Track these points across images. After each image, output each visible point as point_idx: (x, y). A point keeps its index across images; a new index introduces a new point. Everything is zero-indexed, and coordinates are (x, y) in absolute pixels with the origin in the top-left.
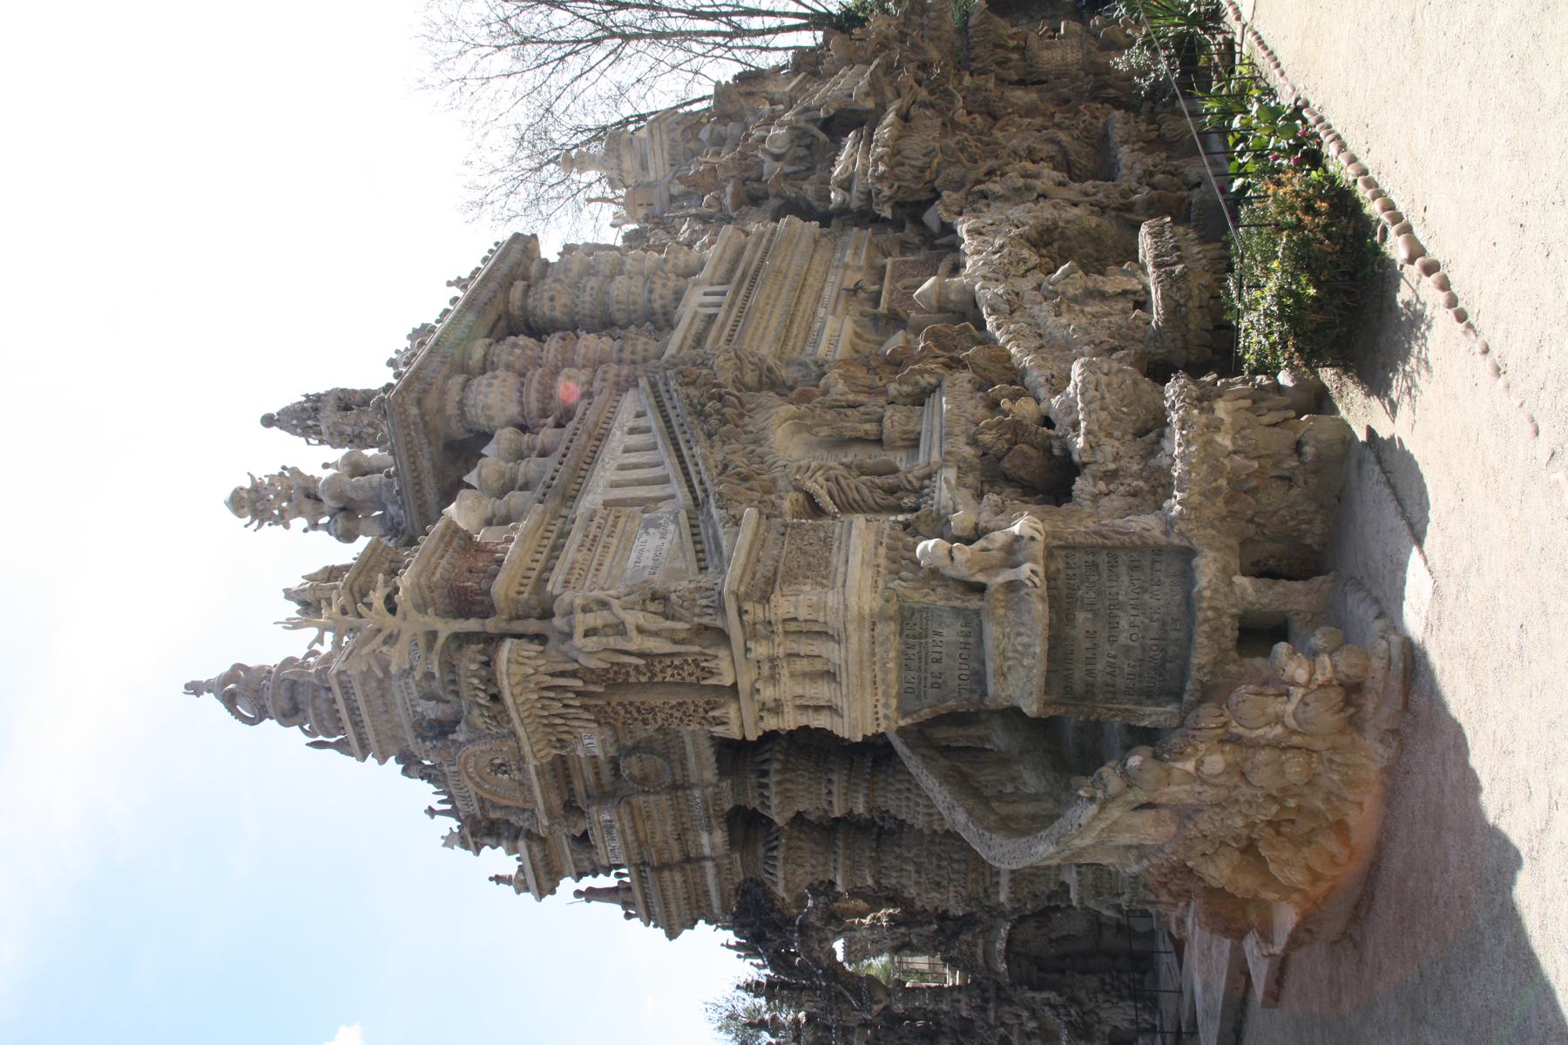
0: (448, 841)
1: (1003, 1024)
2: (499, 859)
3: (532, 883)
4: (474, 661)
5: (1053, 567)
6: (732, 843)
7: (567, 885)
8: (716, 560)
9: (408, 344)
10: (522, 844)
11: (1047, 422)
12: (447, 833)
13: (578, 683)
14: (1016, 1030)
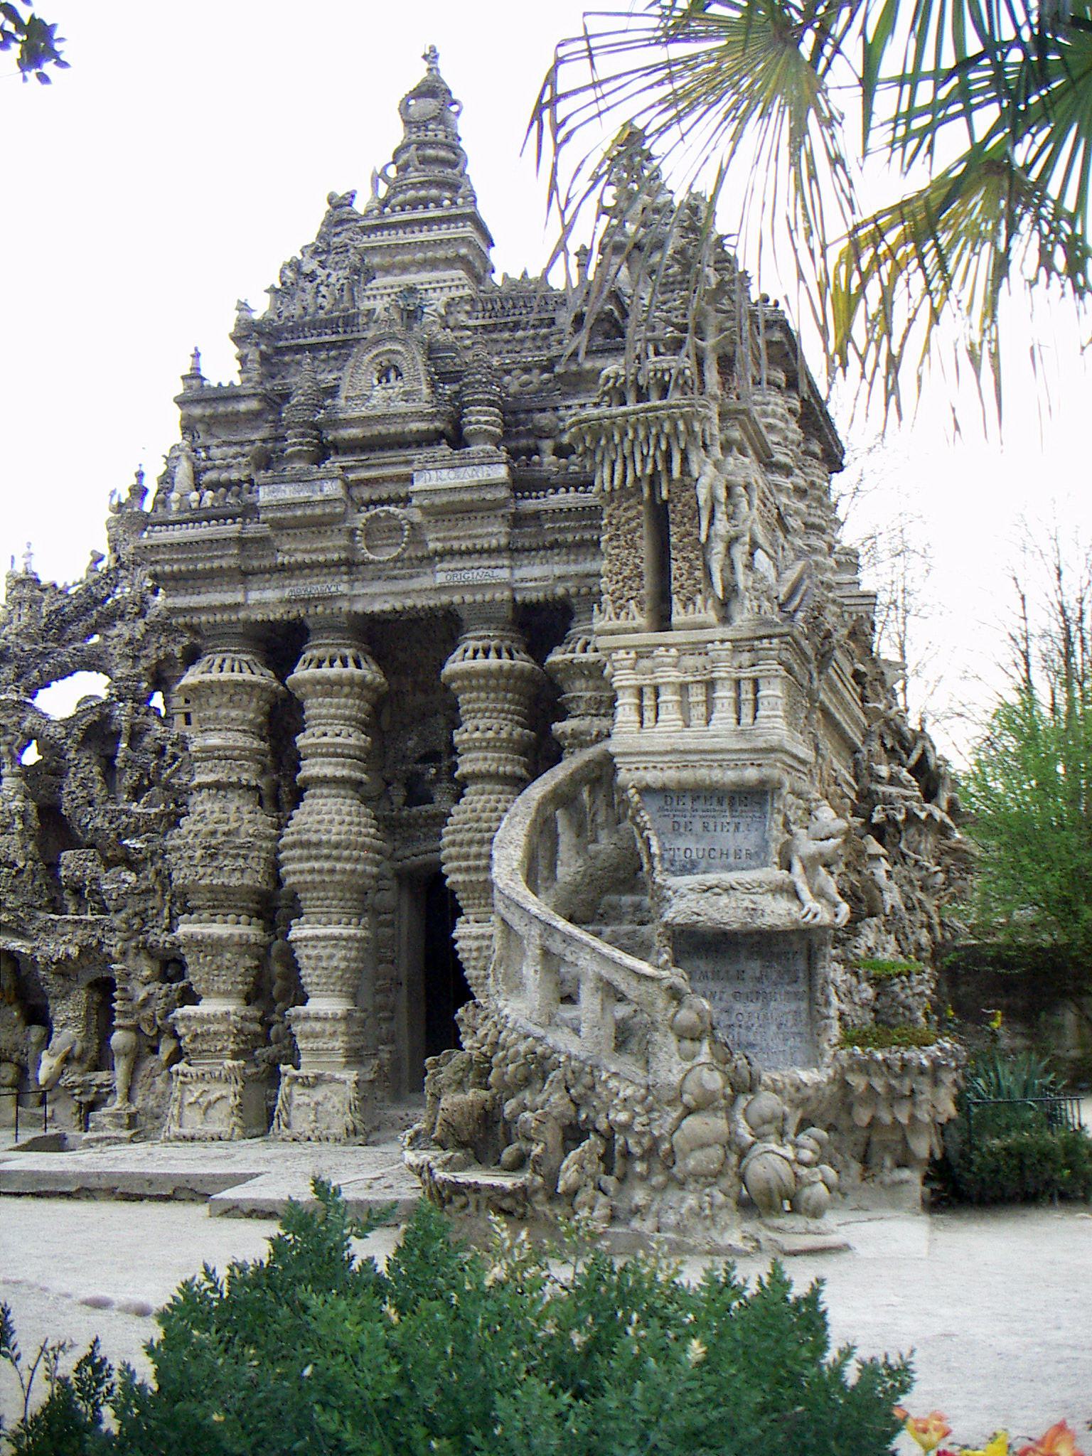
0: (243, 307)
5: (794, 938)
12: (251, 305)
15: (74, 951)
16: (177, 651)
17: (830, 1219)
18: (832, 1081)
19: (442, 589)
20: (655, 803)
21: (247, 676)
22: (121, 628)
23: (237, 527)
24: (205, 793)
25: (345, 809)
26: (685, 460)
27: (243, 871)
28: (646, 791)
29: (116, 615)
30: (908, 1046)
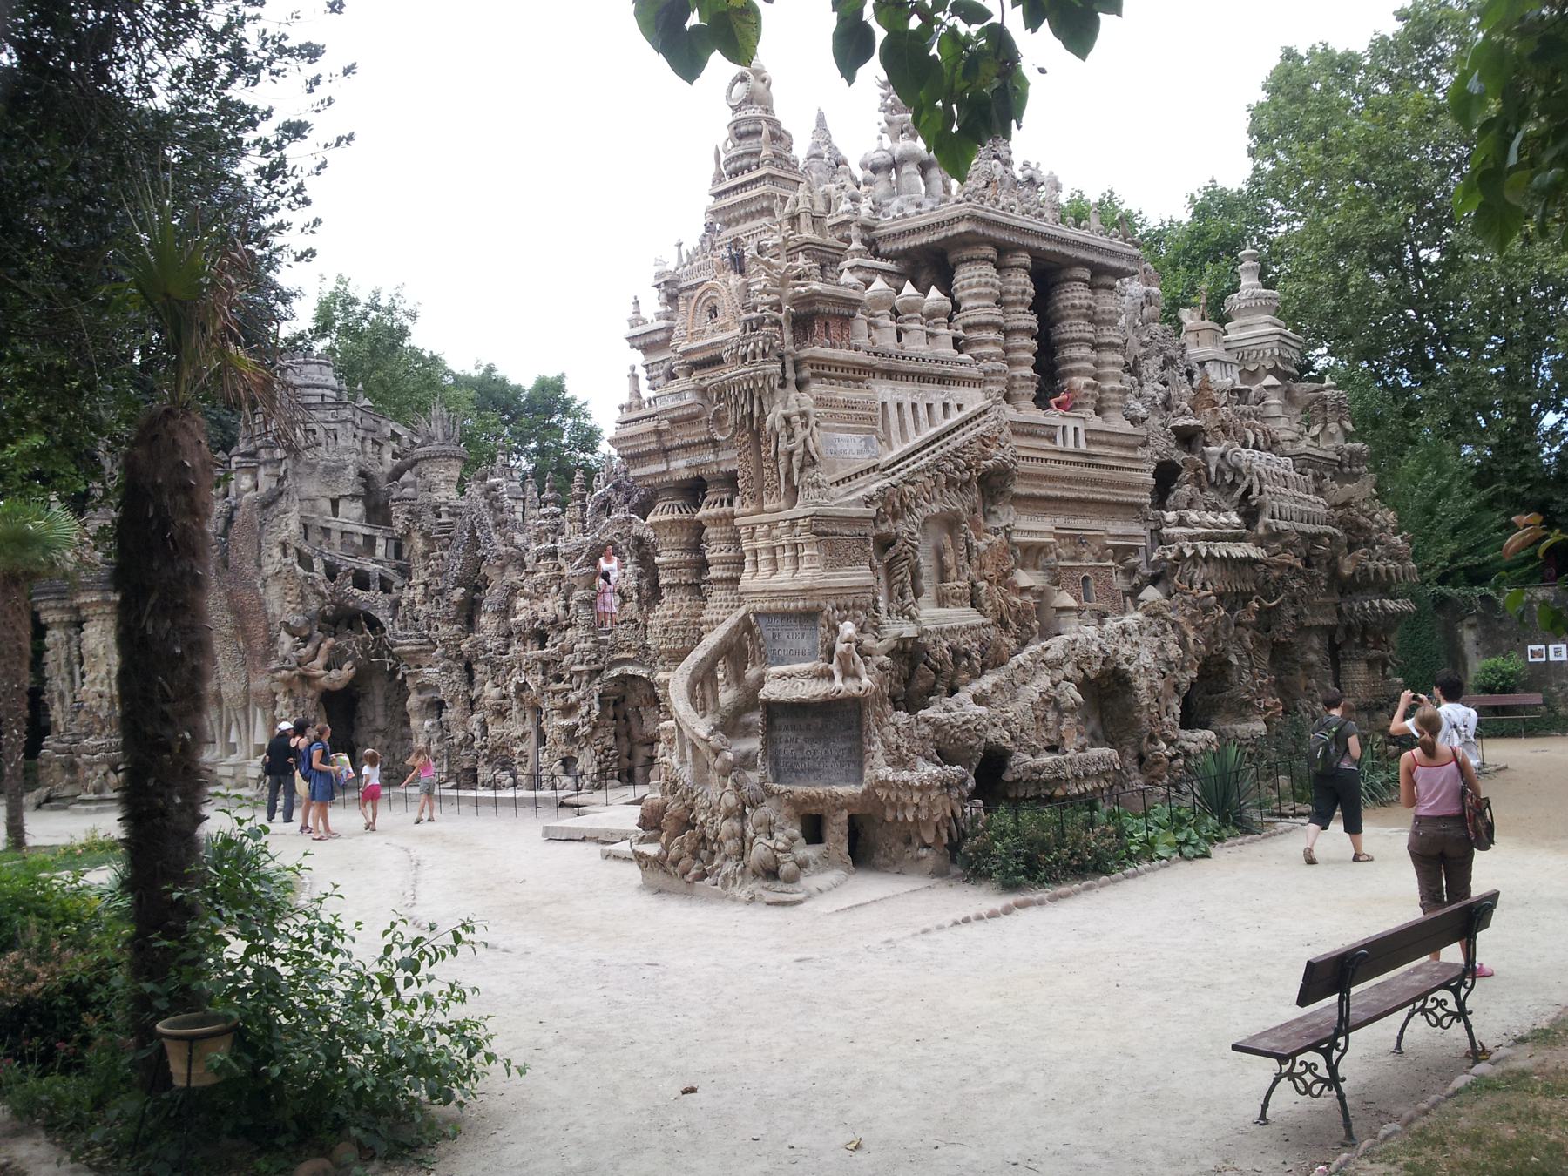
1: (572, 676)
2: (652, 305)
3: (637, 331)
4: (764, 343)
6: (681, 481)
7: (638, 358)
8: (842, 493)
9: (1046, 173)
10: (663, 323)
11: (953, 691)
13: (756, 414)
14: (568, 686)
17: (803, 881)
18: (864, 793)
20: (763, 621)
21: (677, 516)
23: (655, 423)
25: (730, 598)
26: (761, 404)
27: (683, 639)
30: (830, 784)
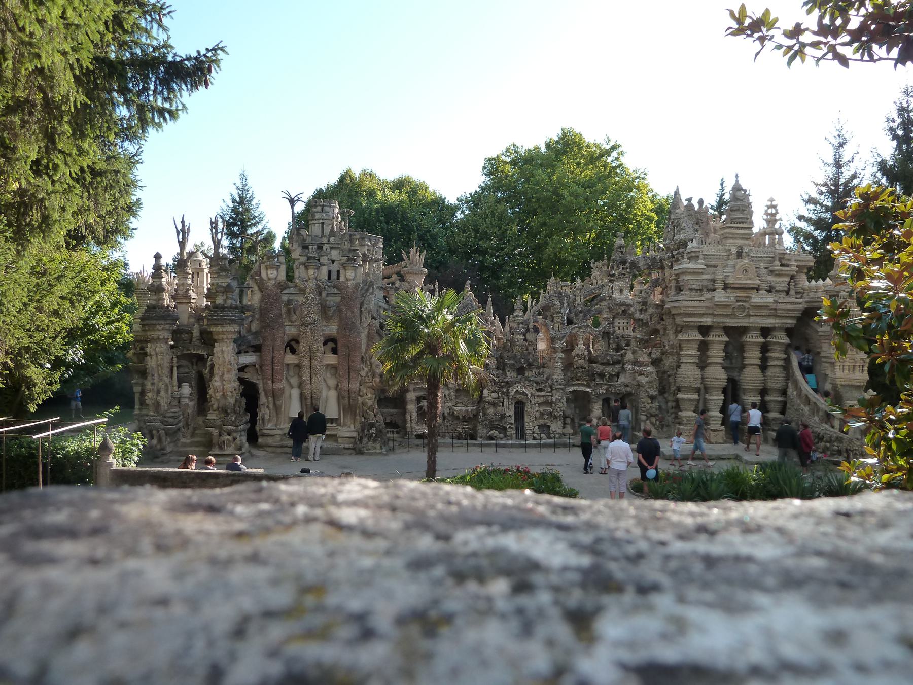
15: (604, 391)
16: (620, 311)
19: (749, 323)
22: (604, 304)
24: (688, 365)
28: (842, 385)
29: (603, 299)
